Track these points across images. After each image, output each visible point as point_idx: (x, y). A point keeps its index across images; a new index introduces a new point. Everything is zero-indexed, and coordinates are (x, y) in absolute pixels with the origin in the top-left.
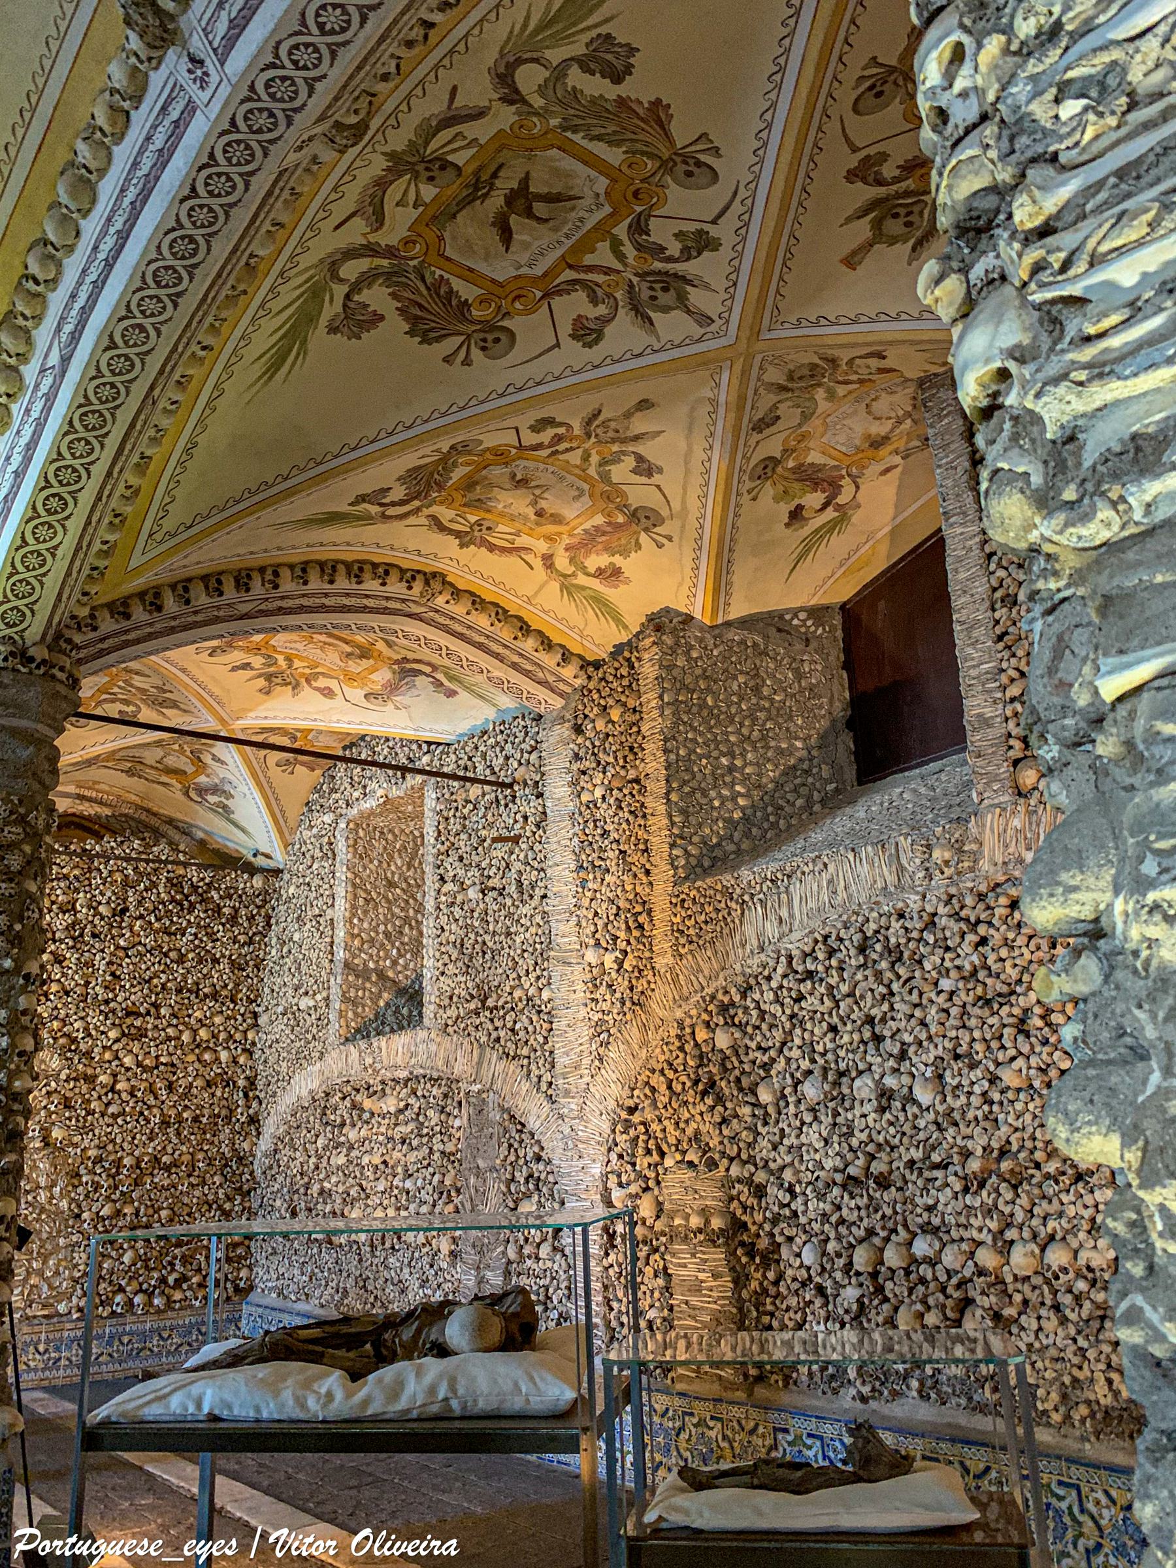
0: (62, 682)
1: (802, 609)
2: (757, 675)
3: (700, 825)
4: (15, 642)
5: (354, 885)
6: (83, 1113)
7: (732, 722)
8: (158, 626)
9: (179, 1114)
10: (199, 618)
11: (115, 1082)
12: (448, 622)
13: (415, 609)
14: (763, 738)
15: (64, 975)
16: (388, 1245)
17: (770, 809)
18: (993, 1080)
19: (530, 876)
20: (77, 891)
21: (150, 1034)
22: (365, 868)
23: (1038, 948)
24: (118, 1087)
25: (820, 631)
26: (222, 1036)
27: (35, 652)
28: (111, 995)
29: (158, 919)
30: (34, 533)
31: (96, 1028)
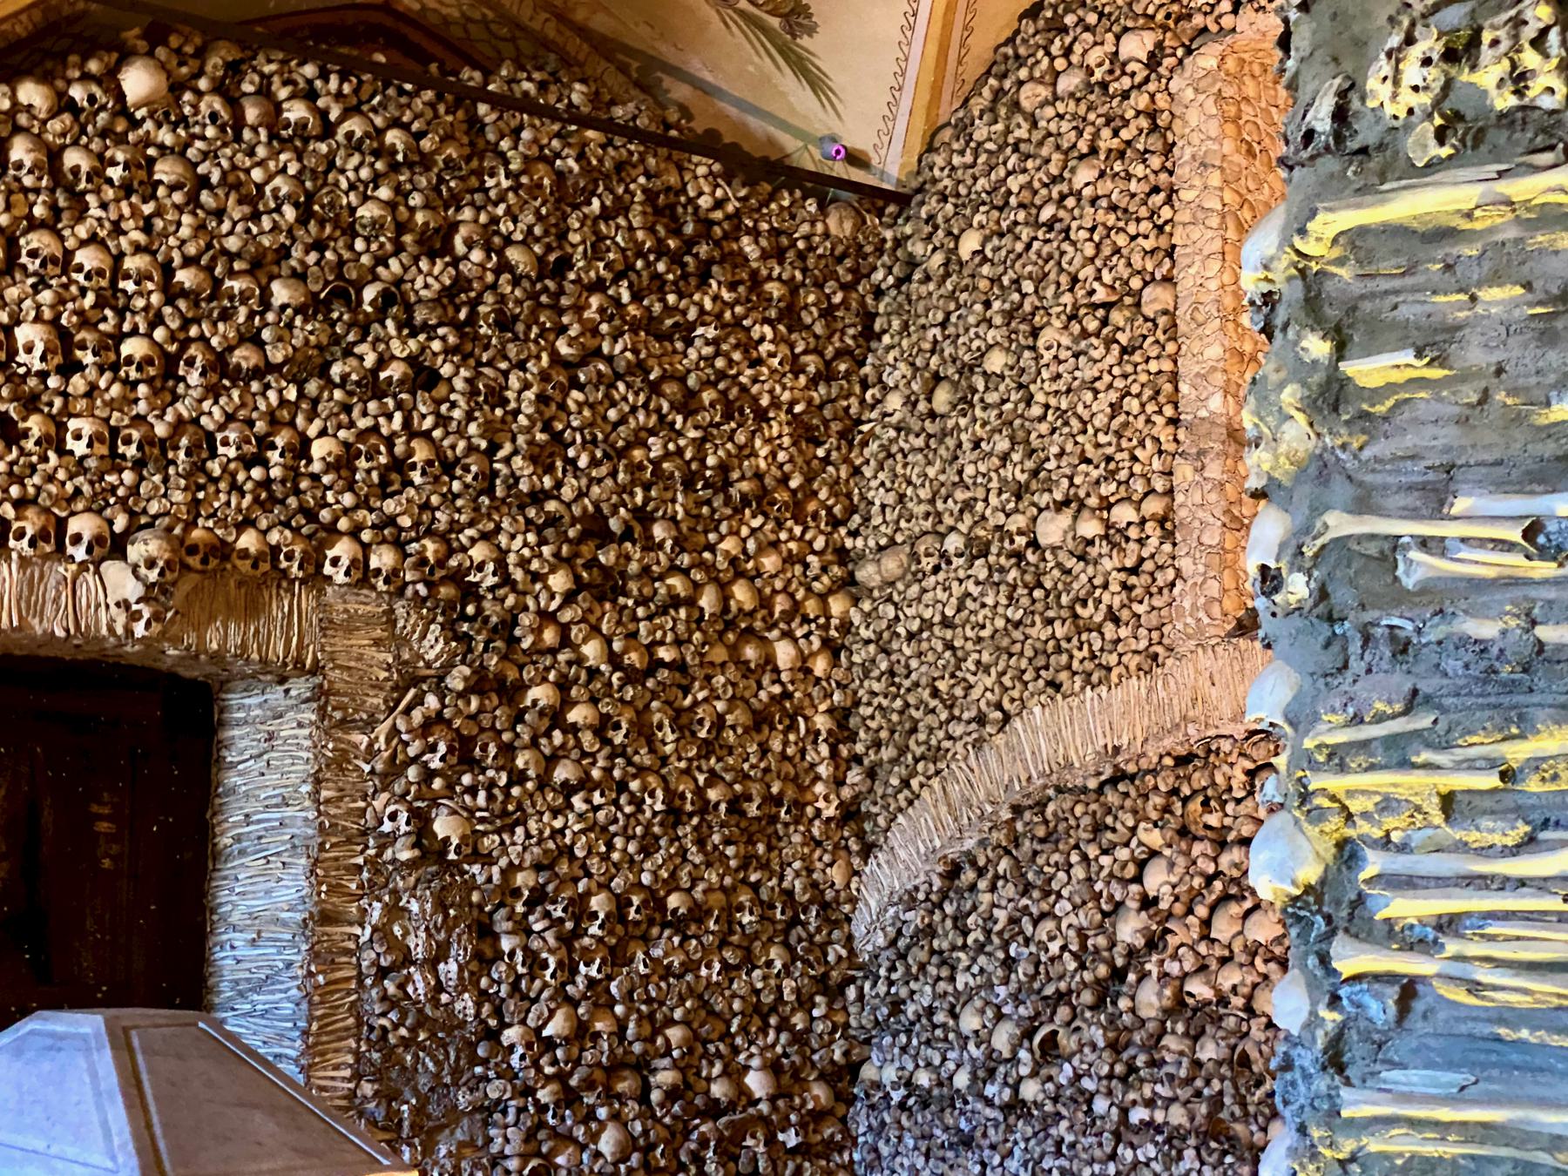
6: (503, 779)
9: (699, 792)
11: (567, 703)
15: (441, 421)
20: (456, 201)
21: (633, 586)
22: (1260, 184)
24: (576, 715)
26: (780, 604)
29: (637, 297)
31: (523, 563)
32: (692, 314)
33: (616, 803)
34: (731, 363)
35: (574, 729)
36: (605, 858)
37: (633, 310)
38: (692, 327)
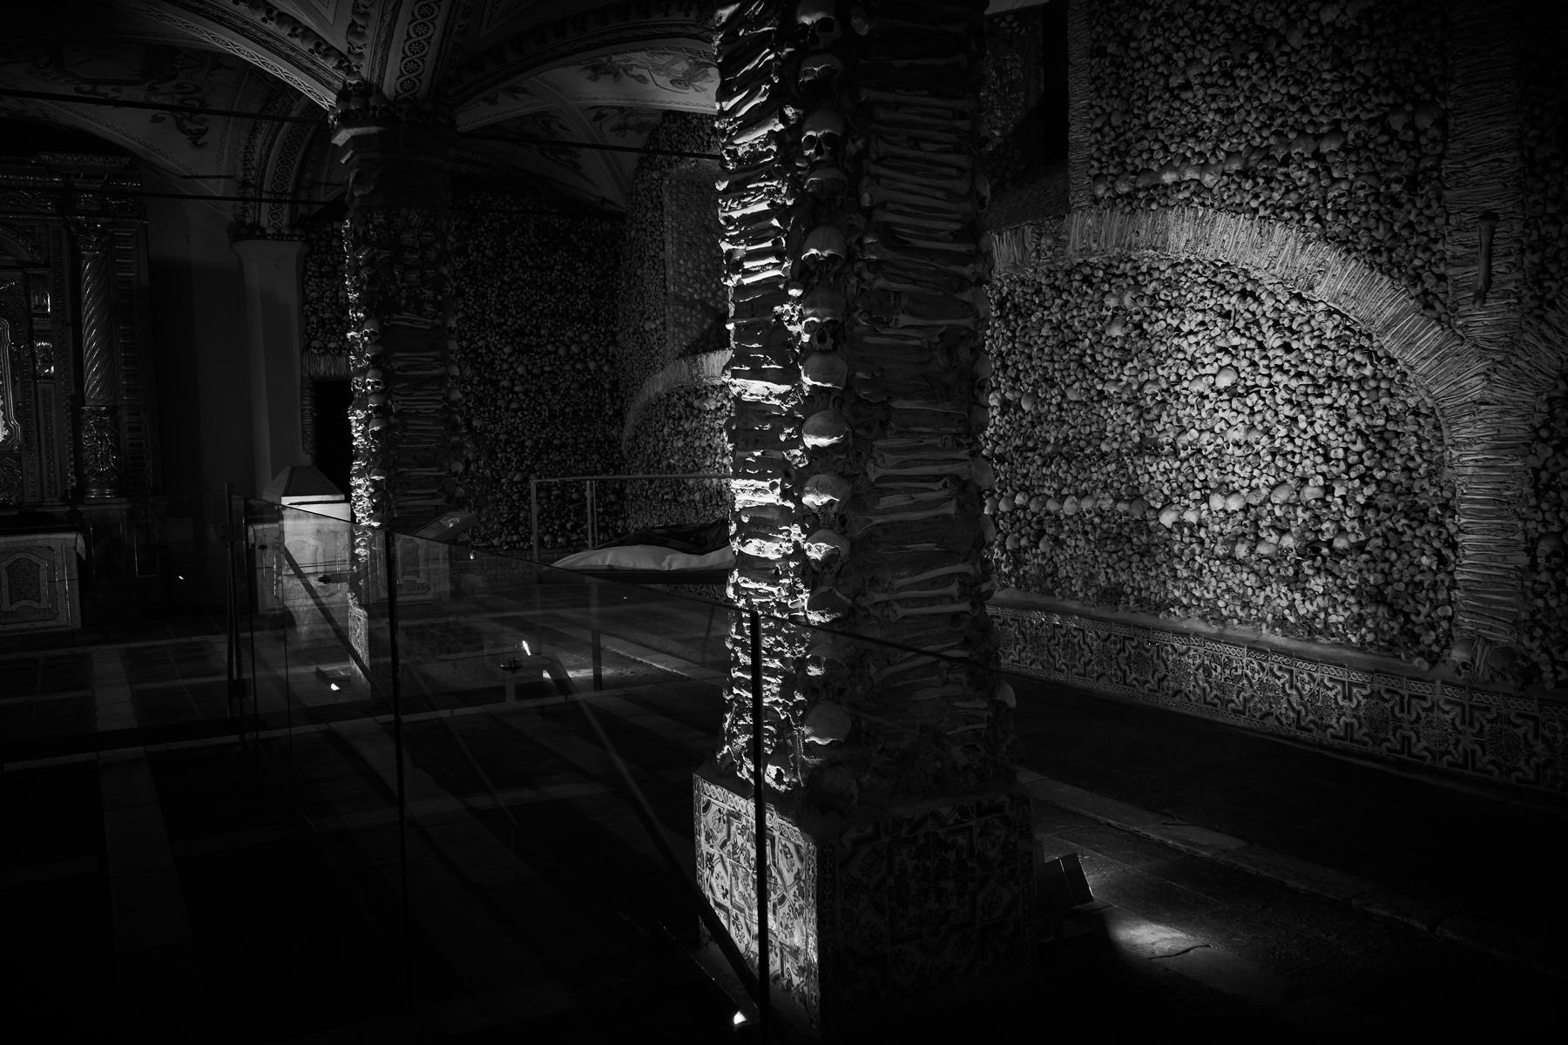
1: (1009, 12)
5: (679, 232)
6: (493, 409)
11: (513, 385)
13: (694, 31)
15: (466, 305)
16: (714, 502)
18: (1064, 396)
23: (1094, 310)
24: (516, 389)
25: (1023, 32)
26: (589, 350)
28: (502, 320)
29: (531, 259)
30: (415, 30)
31: (495, 345)
32: (552, 262)
33: (532, 414)
34: (566, 276)
35: (517, 393)
36: (530, 430)
37: (530, 264)
38: (554, 266)
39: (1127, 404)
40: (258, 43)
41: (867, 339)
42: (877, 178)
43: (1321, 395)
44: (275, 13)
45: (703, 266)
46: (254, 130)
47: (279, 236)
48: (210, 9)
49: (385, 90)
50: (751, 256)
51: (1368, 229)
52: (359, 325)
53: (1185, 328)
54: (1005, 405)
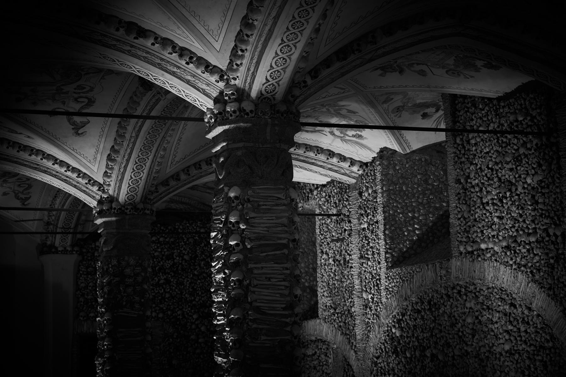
0: (148, 214)
2: (427, 174)
3: (399, 244)
4: (132, 204)
6: (185, 353)
7: (414, 197)
8: (180, 185)
10: (194, 178)
12: (297, 157)
14: (428, 203)
15: (171, 289)
17: (430, 234)
19: (348, 258)
24: (200, 340)
27: (141, 206)
28: (193, 298)
39: (475, 357)
40: (62, 181)
41: (250, 344)
42: (254, 292)
43: (538, 355)
44: (71, 168)
45: (311, 266)
46: (55, 197)
47: (65, 252)
48: (41, 168)
49: (120, 200)
50: (220, 315)
51: (545, 278)
52: (102, 315)
53: (494, 320)
54: (433, 355)
